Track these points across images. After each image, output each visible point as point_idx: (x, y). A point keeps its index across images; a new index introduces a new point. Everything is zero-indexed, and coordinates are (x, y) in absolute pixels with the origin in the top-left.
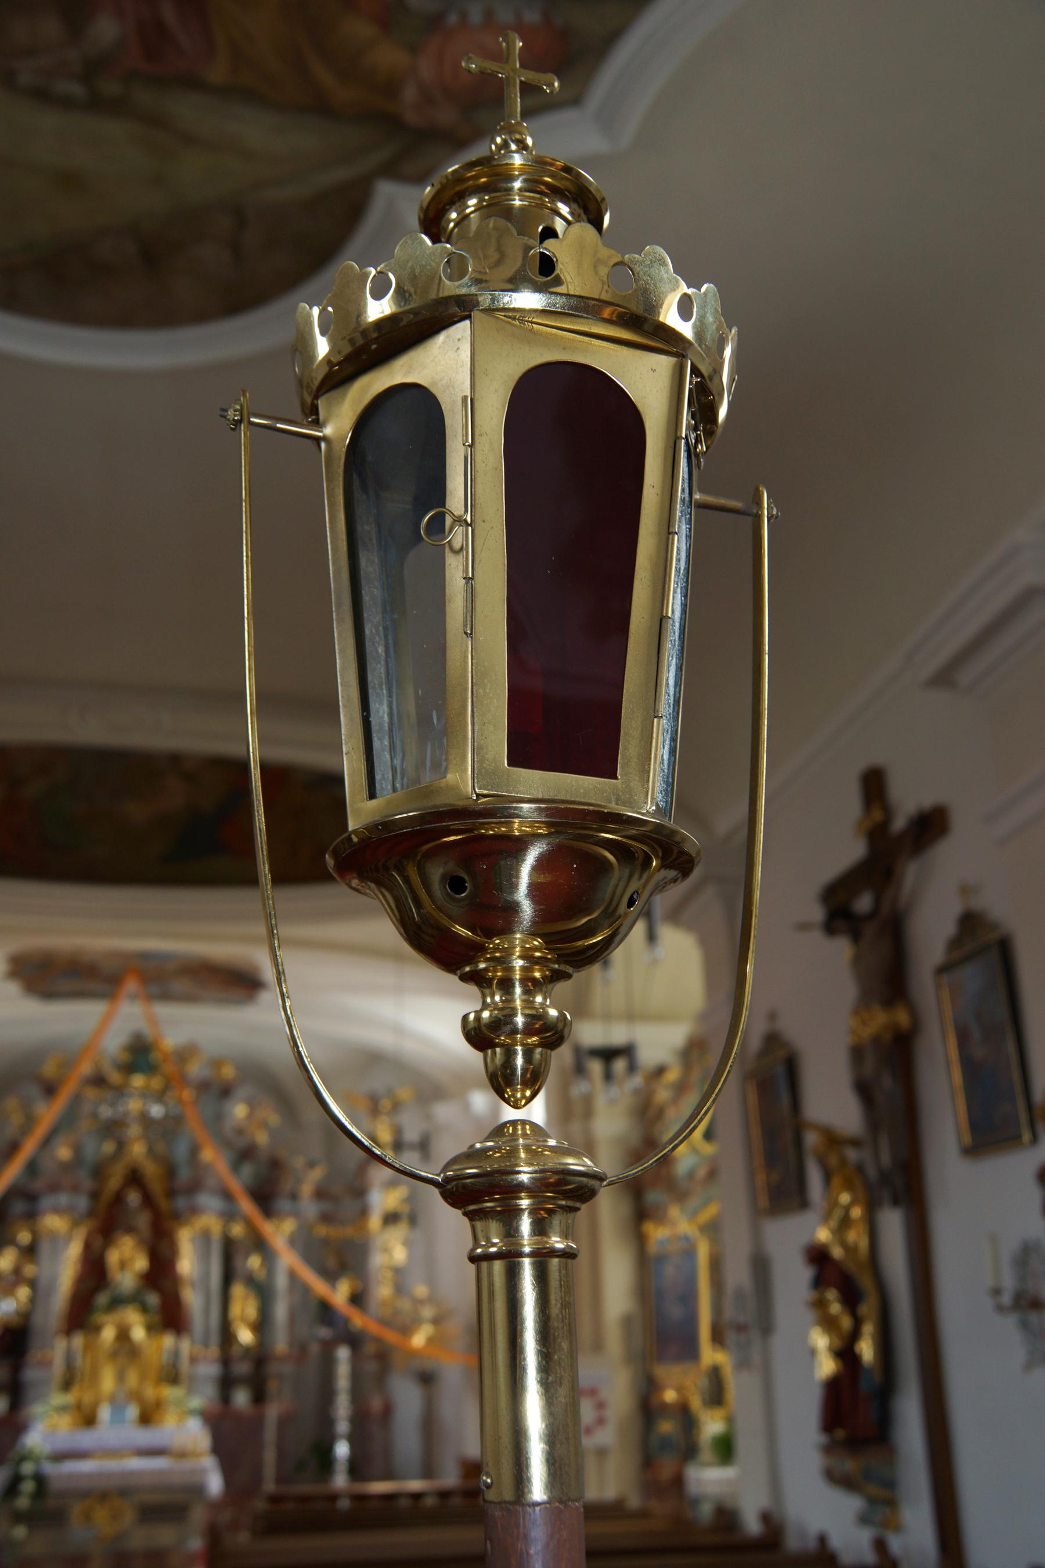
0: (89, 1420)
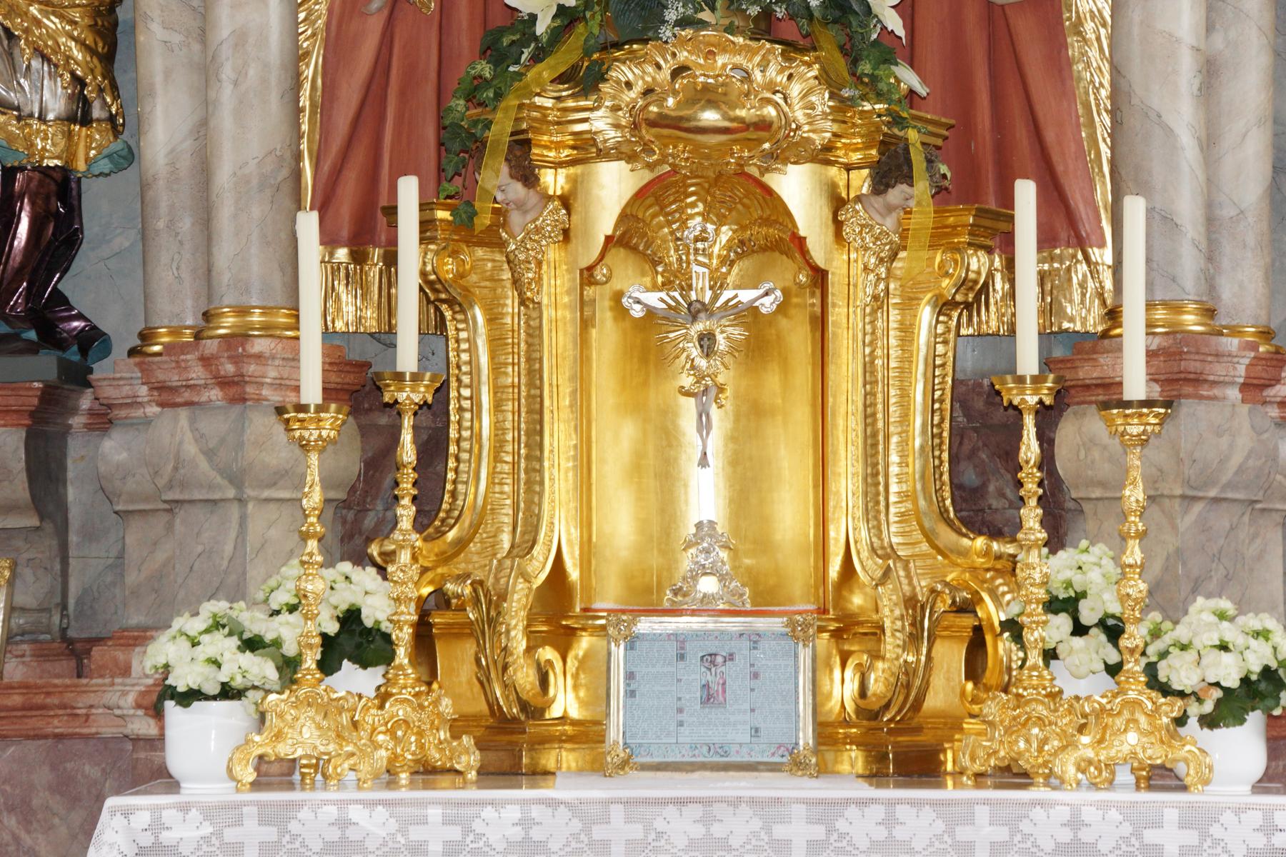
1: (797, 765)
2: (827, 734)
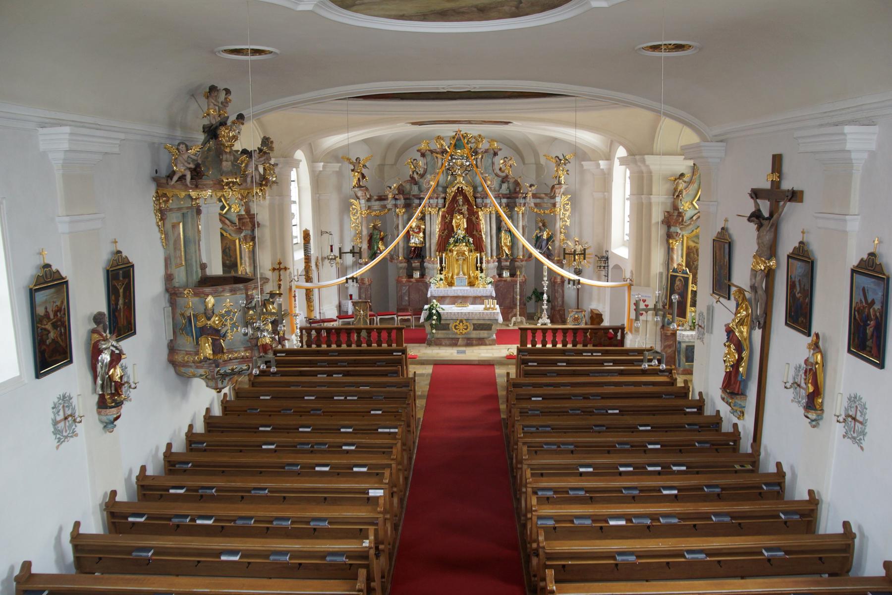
1: (465, 286)
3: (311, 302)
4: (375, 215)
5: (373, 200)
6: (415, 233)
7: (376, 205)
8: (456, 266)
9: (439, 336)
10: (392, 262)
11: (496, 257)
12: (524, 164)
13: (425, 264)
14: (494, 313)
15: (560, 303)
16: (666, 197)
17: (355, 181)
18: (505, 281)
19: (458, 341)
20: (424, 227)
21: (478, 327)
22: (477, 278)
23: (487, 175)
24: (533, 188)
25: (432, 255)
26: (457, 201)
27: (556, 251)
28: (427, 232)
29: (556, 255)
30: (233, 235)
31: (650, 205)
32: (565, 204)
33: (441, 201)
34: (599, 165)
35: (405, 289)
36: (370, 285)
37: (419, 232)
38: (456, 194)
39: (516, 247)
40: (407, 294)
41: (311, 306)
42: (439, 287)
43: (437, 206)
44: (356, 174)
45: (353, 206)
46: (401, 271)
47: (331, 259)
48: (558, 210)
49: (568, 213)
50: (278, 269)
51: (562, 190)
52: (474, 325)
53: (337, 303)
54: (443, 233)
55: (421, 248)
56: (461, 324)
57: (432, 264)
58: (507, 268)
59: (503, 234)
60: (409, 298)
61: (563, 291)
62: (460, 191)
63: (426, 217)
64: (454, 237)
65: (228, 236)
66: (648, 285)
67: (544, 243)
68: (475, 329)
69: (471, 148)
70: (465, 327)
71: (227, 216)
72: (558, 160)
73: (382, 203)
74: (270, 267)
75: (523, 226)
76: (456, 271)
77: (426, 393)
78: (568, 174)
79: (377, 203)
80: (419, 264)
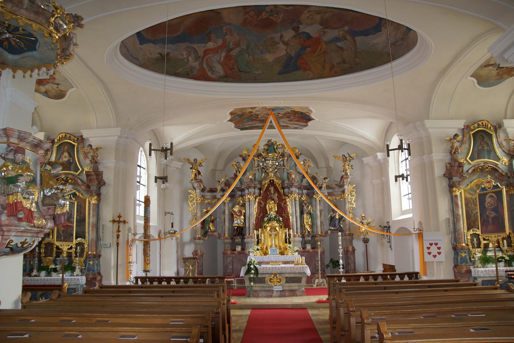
0: (266, 254)
1: (277, 255)
2: (280, 253)
3: (147, 257)
4: (208, 203)
5: (206, 191)
6: (238, 216)
7: (208, 195)
8: (269, 240)
9: (256, 289)
10: (219, 239)
11: (300, 234)
12: (318, 168)
13: (245, 240)
14: (303, 267)
15: (353, 267)
16: (445, 154)
17: (193, 176)
18: (308, 252)
19: (273, 293)
20: (244, 211)
21: (289, 280)
22: (286, 249)
23: (292, 171)
24: (327, 181)
25: (251, 231)
26: (270, 191)
27: (347, 227)
28: (247, 215)
29: (348, 229)
30: (85, 195)
31: (431, 163)
32: (352, 191)
33: (257, 191)
34: (377, 156)
35: (229, 260)
36: (202, 256)
37: (241, 215)
38: (269, 185)
39: (315, 227)
40: (231, 263)
41: (148, 260)
42: (256, 255)
43: (254, 194)
44: (194, 170)
45: (191, 195)
46: (227, 245)
47: (172, 233)
48: (347, 195)
49: (354, 198)
50: (117, 221)
51: (349, 180)
52: (286, 278)
53: (176, 270)
54: (259, 215)
55: (242, 227)
56: (275, 277)
57: (250, 240)
58: (309, 242)
59: (305, 216)
60: (233, 267)
61: (354, 258)
62: (272, 183)
63: (246, 204)
64: (268, 217)
65: (80, 195)
66: (438, 230)
67: (337, 222)
68: (287, 282)
69: (279, 153)
70: (279, 280)
71: (80, 177)
72: (344, 158)
73: (213, 194)
74: (111, 219)
75: (320, 210)
76: (270, 244)
77: (244, 328)
78: (352, 168)
79: (209, 194)
80: (240, 240)
